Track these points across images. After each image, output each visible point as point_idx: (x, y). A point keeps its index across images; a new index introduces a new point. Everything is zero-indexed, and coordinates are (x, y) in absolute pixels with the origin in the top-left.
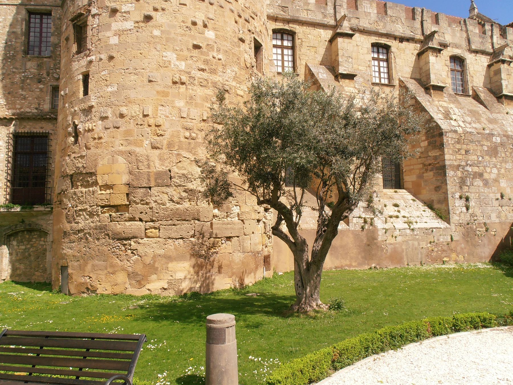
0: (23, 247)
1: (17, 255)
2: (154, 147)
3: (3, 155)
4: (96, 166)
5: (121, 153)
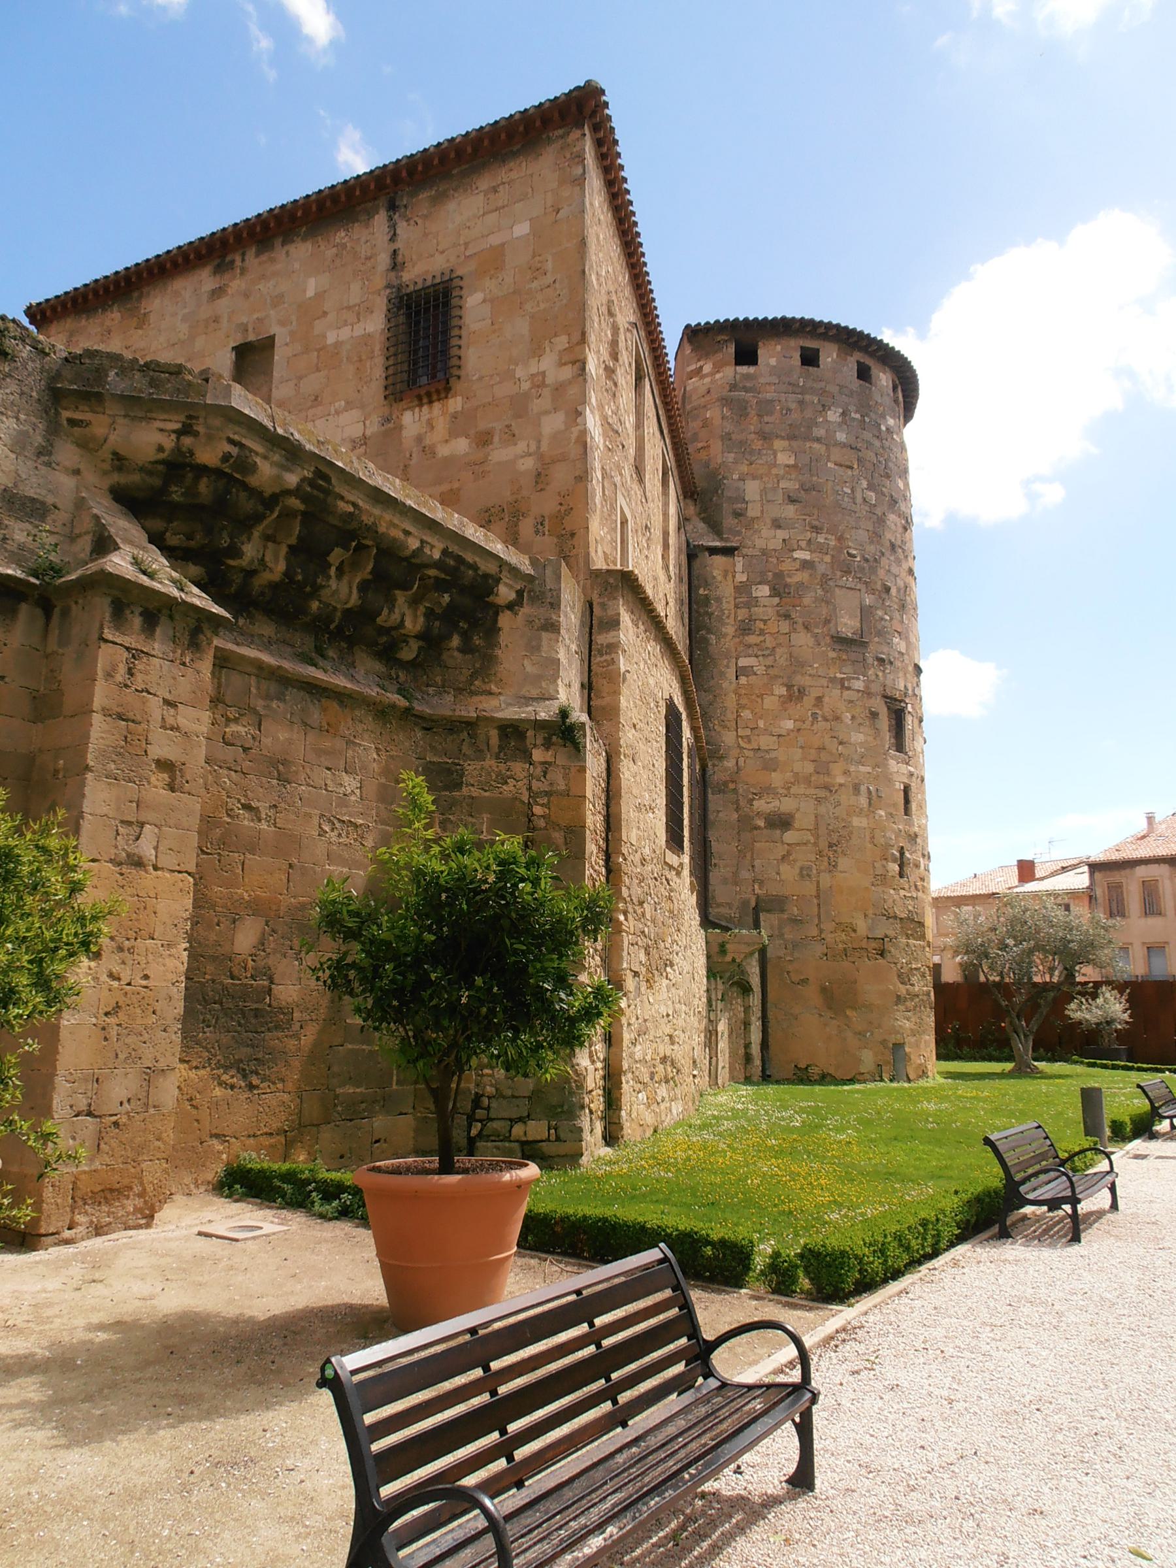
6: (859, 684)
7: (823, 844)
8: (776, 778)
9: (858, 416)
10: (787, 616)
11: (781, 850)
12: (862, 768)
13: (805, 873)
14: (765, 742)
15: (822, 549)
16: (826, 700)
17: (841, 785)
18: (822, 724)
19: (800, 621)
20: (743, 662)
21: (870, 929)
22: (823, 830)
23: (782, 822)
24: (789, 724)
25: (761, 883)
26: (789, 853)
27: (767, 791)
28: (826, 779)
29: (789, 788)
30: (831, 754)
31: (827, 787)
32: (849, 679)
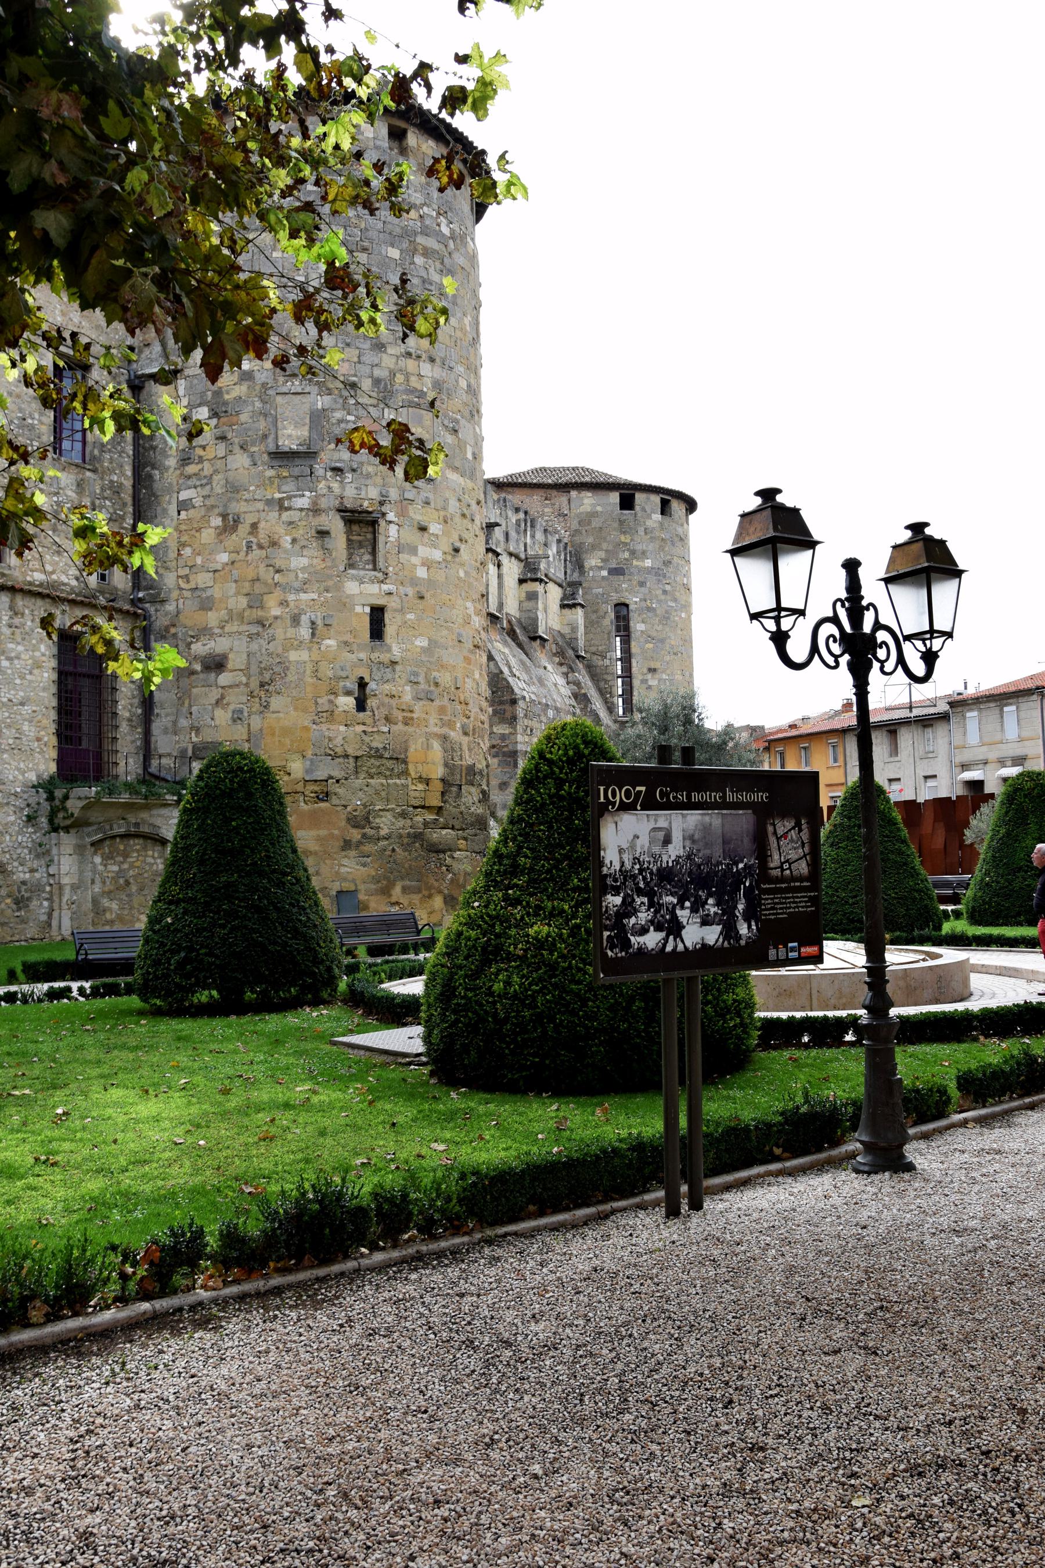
0: (116, 868)
1: (104, 883)
2: (466, 734)
3: (46, 675)
4: (406, 750)
5: (437, 736)
6: (303, 502)
7: (254, 684)
8: (212, 618)
10: (223, 438)
11: (215, 694)
12: (303, 596)
13: (237, 718)
14: (202, 579)
16: (262, 525)
17: (276, 618)
18: (257, 553)
19: (236, 440)
20: (184, 495)
21: (307, 771)
22: (254, 669)
24: (224, 558)
25: (198, 730)
26: (223, 697)
27: (204, 632)
28: (260, 613)
29: (223, 628)
30: (266, 584)
31: (260, 623)
32: (289, 498)
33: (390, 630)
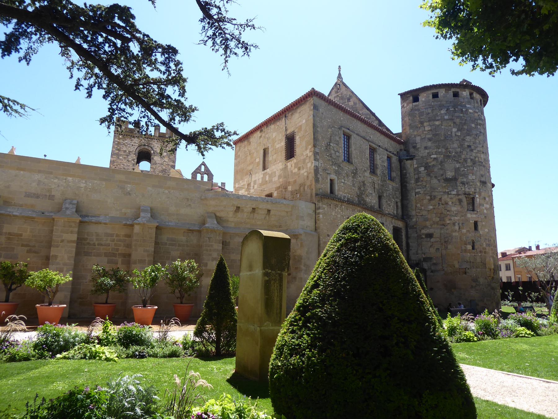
8: (428, 223)
9: (453, 109)
12: (456, 218)
14: (424, 213)
15: (440, 153)
20: (417, 190)
23: (430, 236)
32: (451, 191)
33: (479, 227)
